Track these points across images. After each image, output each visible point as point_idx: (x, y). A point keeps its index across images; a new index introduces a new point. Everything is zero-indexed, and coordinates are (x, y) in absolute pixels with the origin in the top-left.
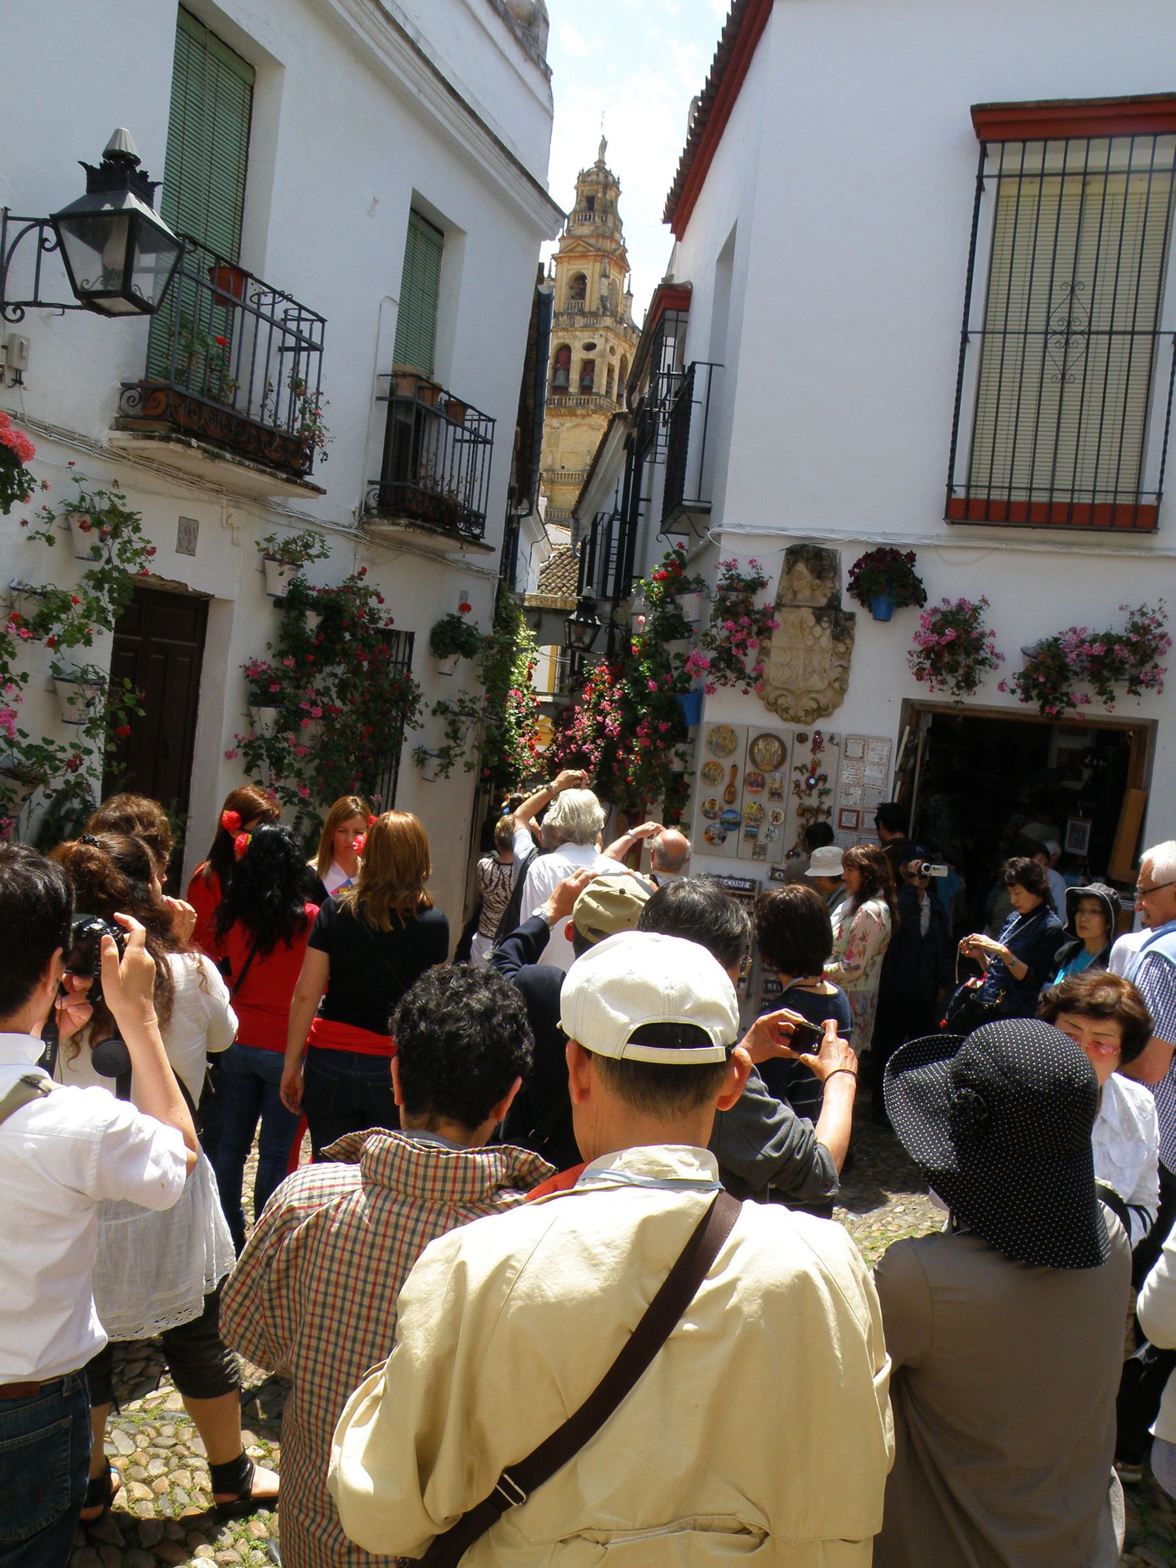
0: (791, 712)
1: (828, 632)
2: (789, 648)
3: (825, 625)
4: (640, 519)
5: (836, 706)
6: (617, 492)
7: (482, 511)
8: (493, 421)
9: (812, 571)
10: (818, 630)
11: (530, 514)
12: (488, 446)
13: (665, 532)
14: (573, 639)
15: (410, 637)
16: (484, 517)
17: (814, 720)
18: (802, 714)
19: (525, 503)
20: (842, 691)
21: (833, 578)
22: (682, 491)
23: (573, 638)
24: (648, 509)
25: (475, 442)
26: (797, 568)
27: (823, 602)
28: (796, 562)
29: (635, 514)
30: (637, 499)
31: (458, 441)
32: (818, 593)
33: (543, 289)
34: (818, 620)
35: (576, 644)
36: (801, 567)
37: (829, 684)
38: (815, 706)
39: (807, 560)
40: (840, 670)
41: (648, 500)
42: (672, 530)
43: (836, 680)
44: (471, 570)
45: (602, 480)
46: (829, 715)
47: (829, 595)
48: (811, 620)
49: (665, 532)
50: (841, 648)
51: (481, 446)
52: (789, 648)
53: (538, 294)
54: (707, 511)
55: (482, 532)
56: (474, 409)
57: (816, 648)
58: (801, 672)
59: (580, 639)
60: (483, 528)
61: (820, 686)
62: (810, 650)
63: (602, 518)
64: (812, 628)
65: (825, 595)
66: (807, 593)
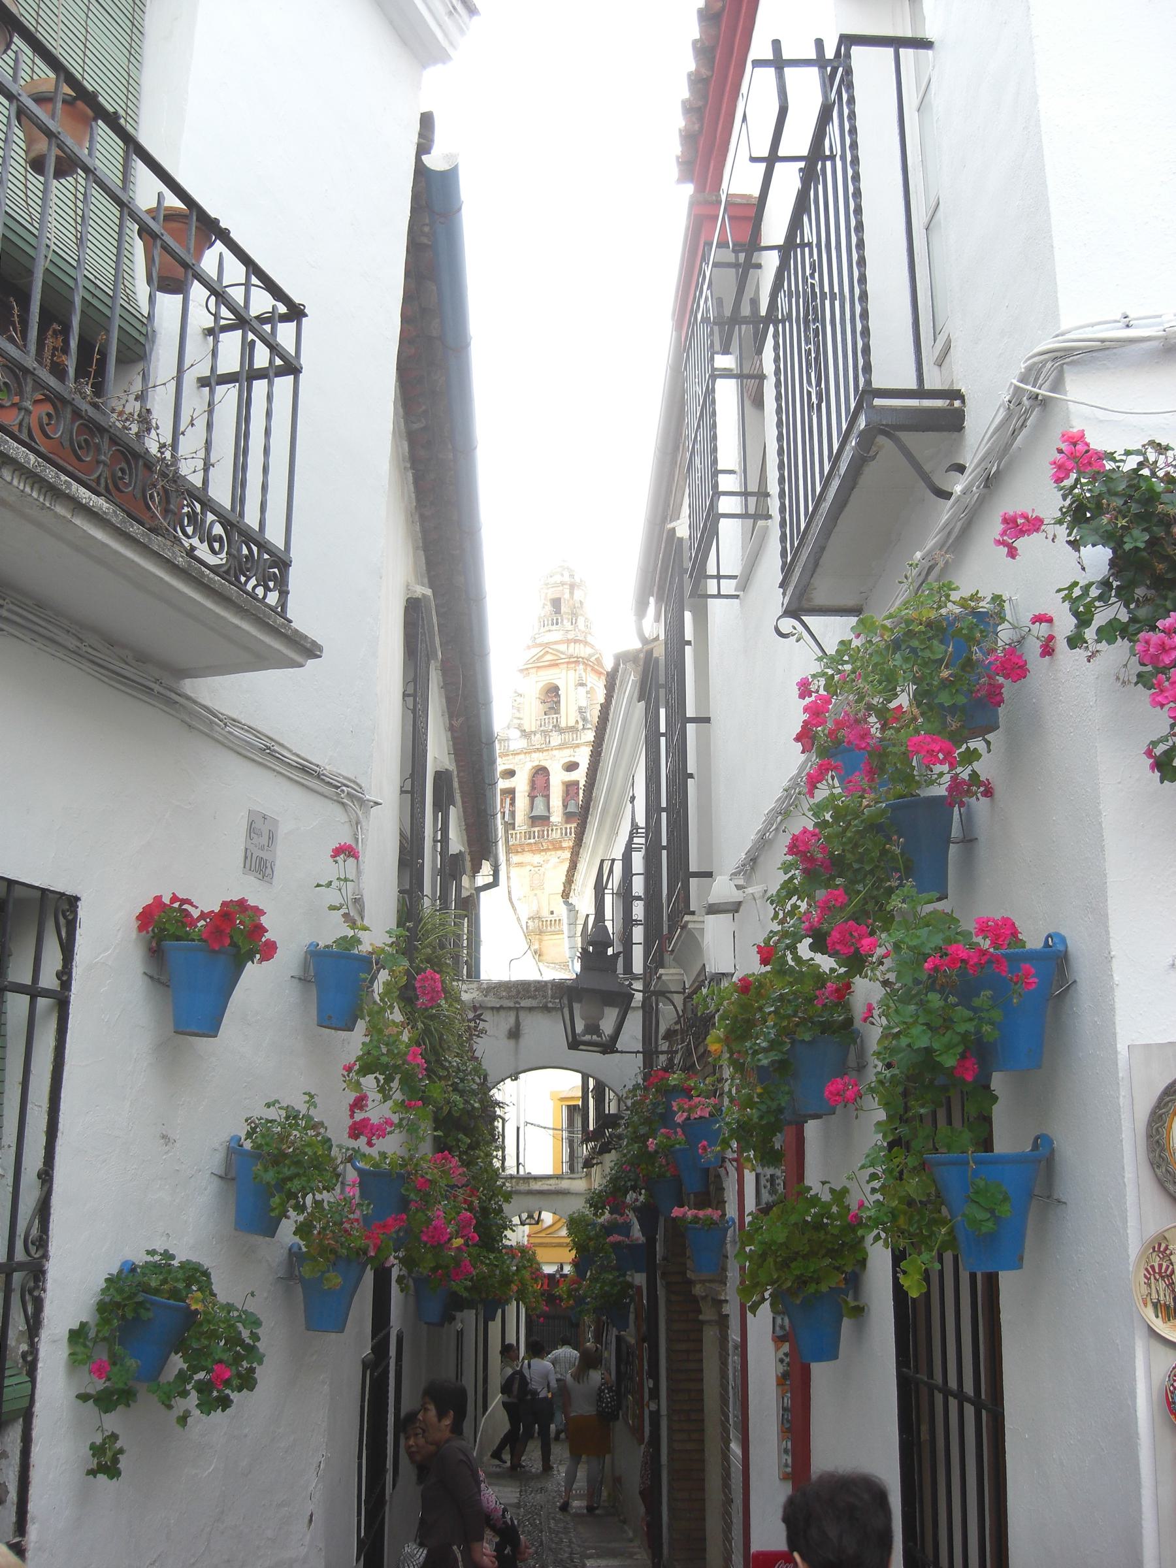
6: (633, 798)
7: (275, 535)
8: (296, 313)
11: (495, 884)
12: (284, 384)
13: (793, 611)
14: (579, 1028)
15: (60, 910)
19: (486, 867)
23: (579, 1028)
25: (247, 376)
29: (680, 776)
35: (587, 1038)
42: (820, 597)
44: (272, 754)
45: (603, 810)
51: (260, 386)
55: (283, 602)
59: (593, 1028)
60: (284, 594)
63: (611, 871)
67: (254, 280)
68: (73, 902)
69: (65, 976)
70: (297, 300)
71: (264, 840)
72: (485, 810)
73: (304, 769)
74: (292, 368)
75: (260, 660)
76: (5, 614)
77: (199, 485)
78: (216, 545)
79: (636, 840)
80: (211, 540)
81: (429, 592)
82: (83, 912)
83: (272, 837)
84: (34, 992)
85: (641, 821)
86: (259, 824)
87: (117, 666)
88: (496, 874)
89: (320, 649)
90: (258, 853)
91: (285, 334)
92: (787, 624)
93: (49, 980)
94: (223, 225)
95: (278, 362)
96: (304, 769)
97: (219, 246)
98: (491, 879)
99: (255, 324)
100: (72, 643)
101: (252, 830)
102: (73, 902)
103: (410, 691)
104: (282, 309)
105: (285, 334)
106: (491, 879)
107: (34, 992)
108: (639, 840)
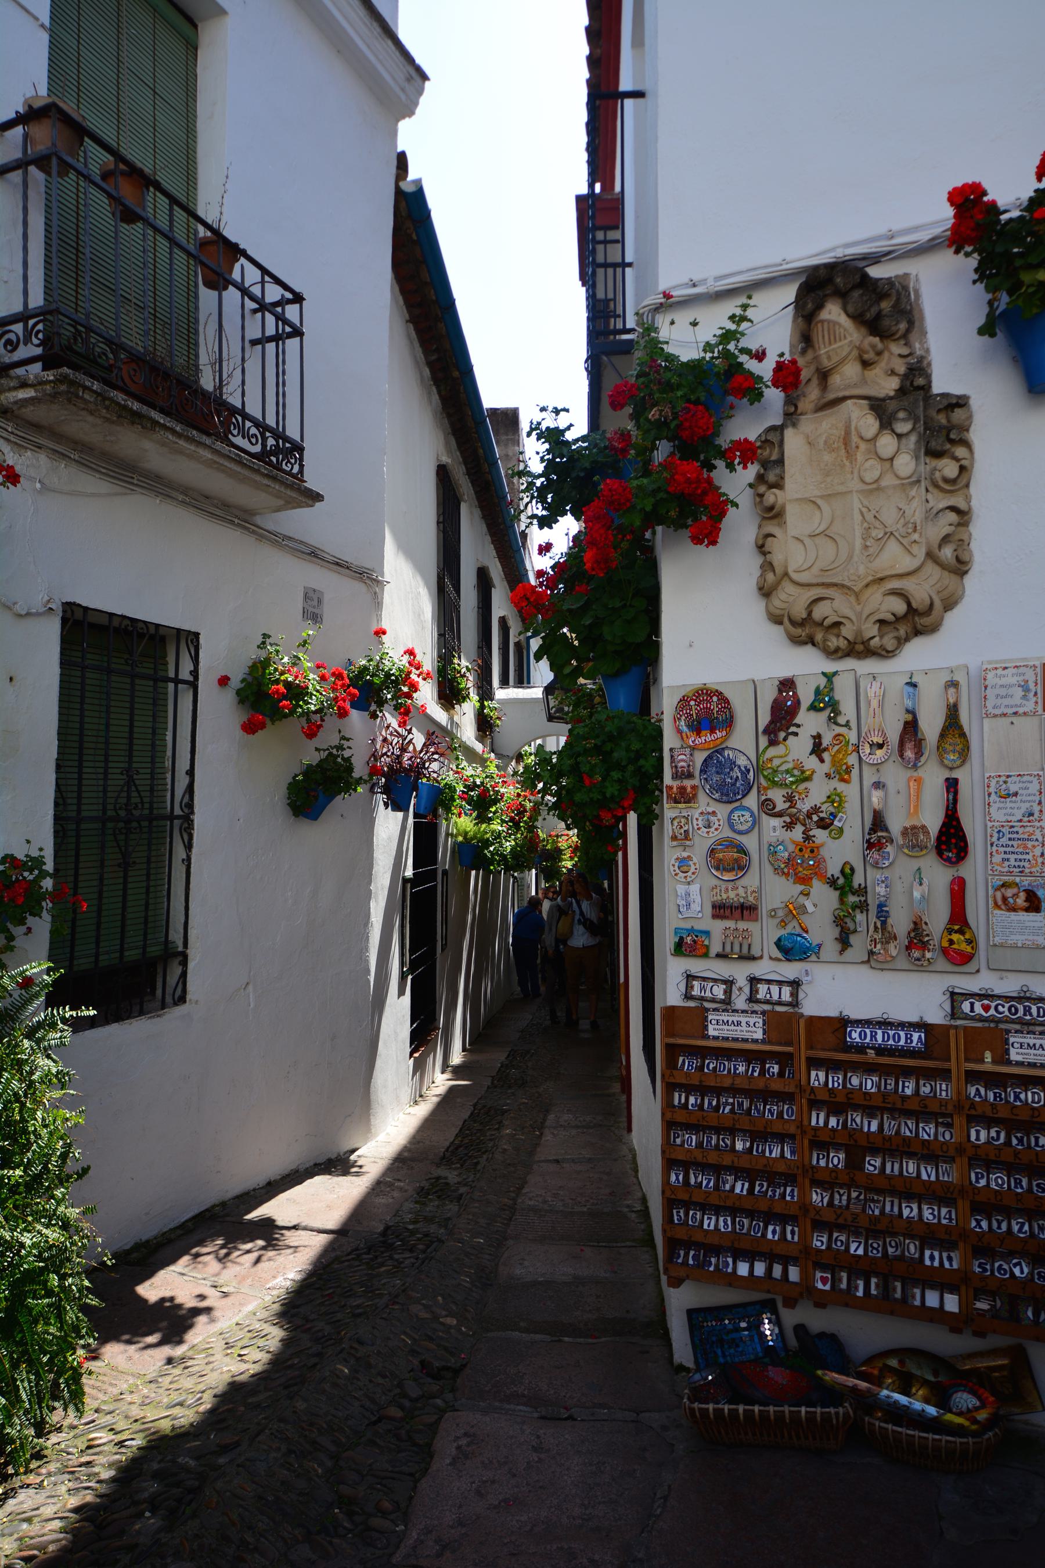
0: (847, 631)
1: (913, 438)
2: (827, 497)
3: (903, 427)
5: (950, 604)
7: (293, 432)
8: (298, 299)
9: (858, 318)
10: (887, 443)
16: (301, 449)
17: (902, 642)
18: (871, 630)
20: (960, 567)
21: (905, 336)
25: (277, 338)
26: (824, 315)
27: (889, 386)
28: (820, 307)
31: (254, 343)
32: (877, 372)
33: (406, 187)
34: (886, 422)
36: (833, 312)
37: (930, 555)
38: (899, 607)
39: (842, 295)
40: (953, 517)
43: (946, 539)
44: (316, 556)
46: (932, 629)
47: (902, 369)
48: (869, 424)
50: (950, 469)
52: (822, 497)
53: (399, 193)
56: (244, 253)
57: (888, 481)
58: (858, 543)
60: (301, 466)
61: (907, 563)
62: (875, 488)
64: (874, 439)
65: (893, 373)
66: (851, 370)
67: (267, 278)
68: (197, 635)
69: (195, 673)
70: (297, 290)
71: (315, 603)
73: (337, 564)
74: (297, 333)
75: (291, 504)
76: (135, 482)
77: (240, 407)
78: (254, 440)
80: (249, 437)
82: (202, 640)
83: (320, 601)
84: (177, 681)
86: (311, 594)
87: (212, 509)
89: (322, 497)
90: (311, 609)
91: (292, 312)
93: (185, 674)
94: (241, 247)
95: (288, 329)
96: (337, 564)
97: (243, 260)
99: (271, 309)
100: (181, 497)
101: (306, 597)
102: (197, 635)
103: (441, 520)
104: (289, 295)
105: (292, 312)
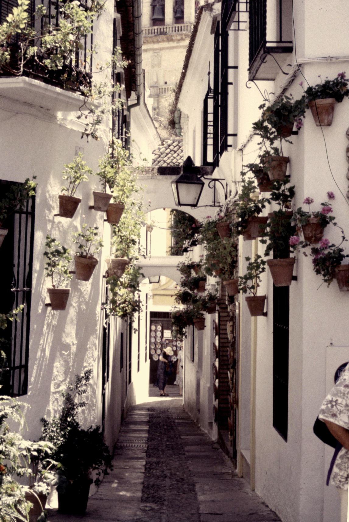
4: (230, 88)
7: (88, 70)
11: (138, 104)
13: (253, 78)
19: (133, 95)
22: (264, 35)
24: (236, 76)
29: (226, 83)
30: (226, 67)
41: (236, 67)
49: (253, 78)
54: (289, 50)
72: (135, 72)
79: (210, 94)
81: (119, 16)
85: (212, 87)
88: (138, 99)
92: (251, 84)
93: (30, 210)
98: (136, 102)
106: (136, 102)
107: (27, 213)
108: (211, 94)
